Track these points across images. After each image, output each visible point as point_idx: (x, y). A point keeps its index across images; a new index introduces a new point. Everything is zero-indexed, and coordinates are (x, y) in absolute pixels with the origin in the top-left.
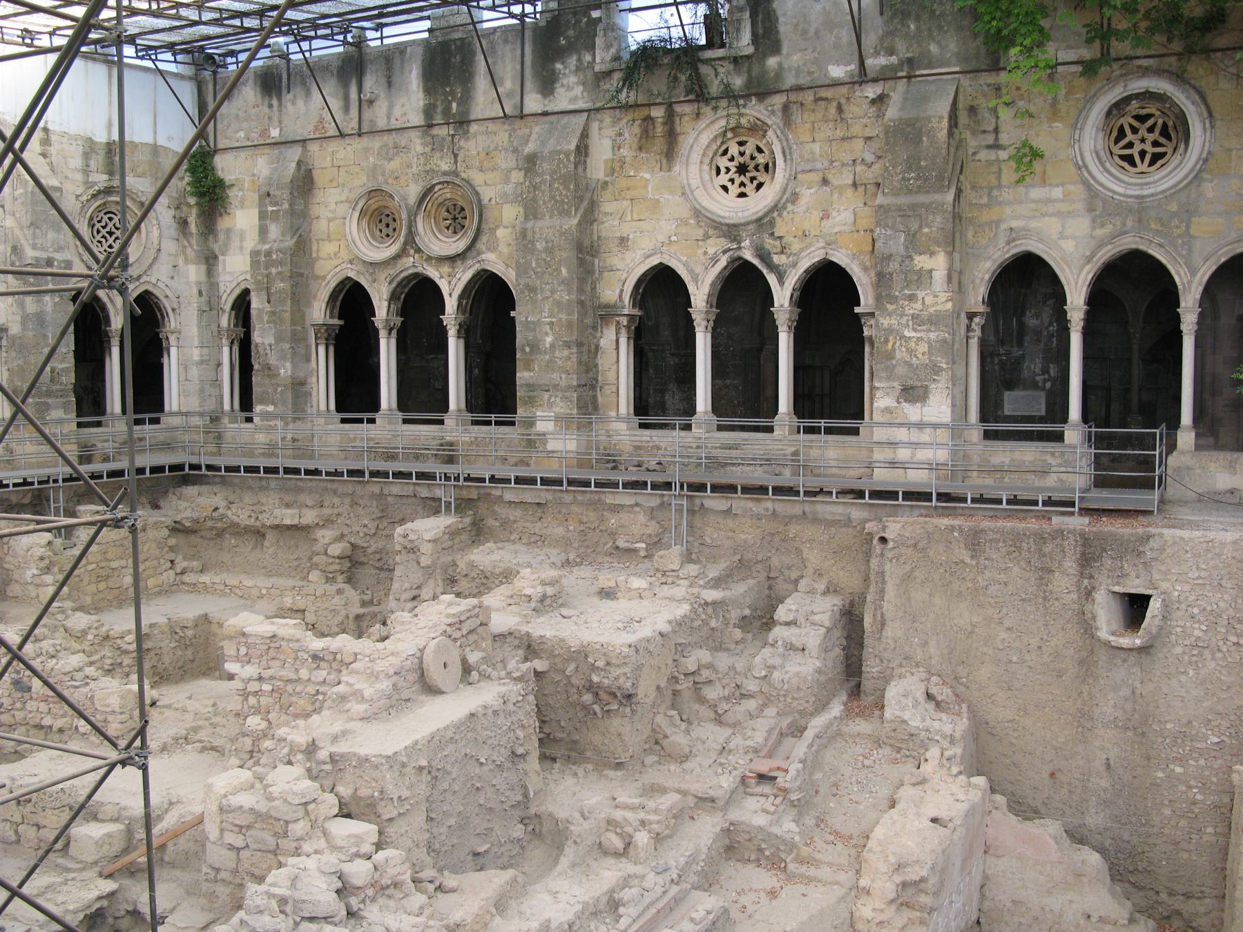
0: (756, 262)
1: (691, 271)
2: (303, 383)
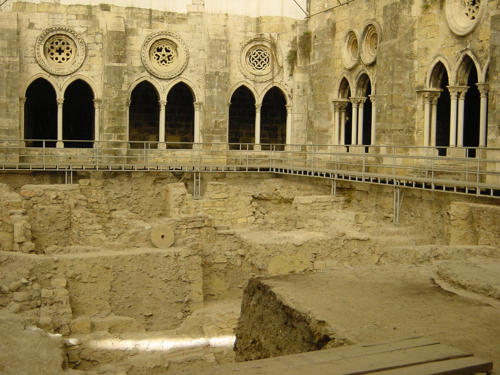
0: (472, 56)
1: (449, 64)
2: (325, 131)
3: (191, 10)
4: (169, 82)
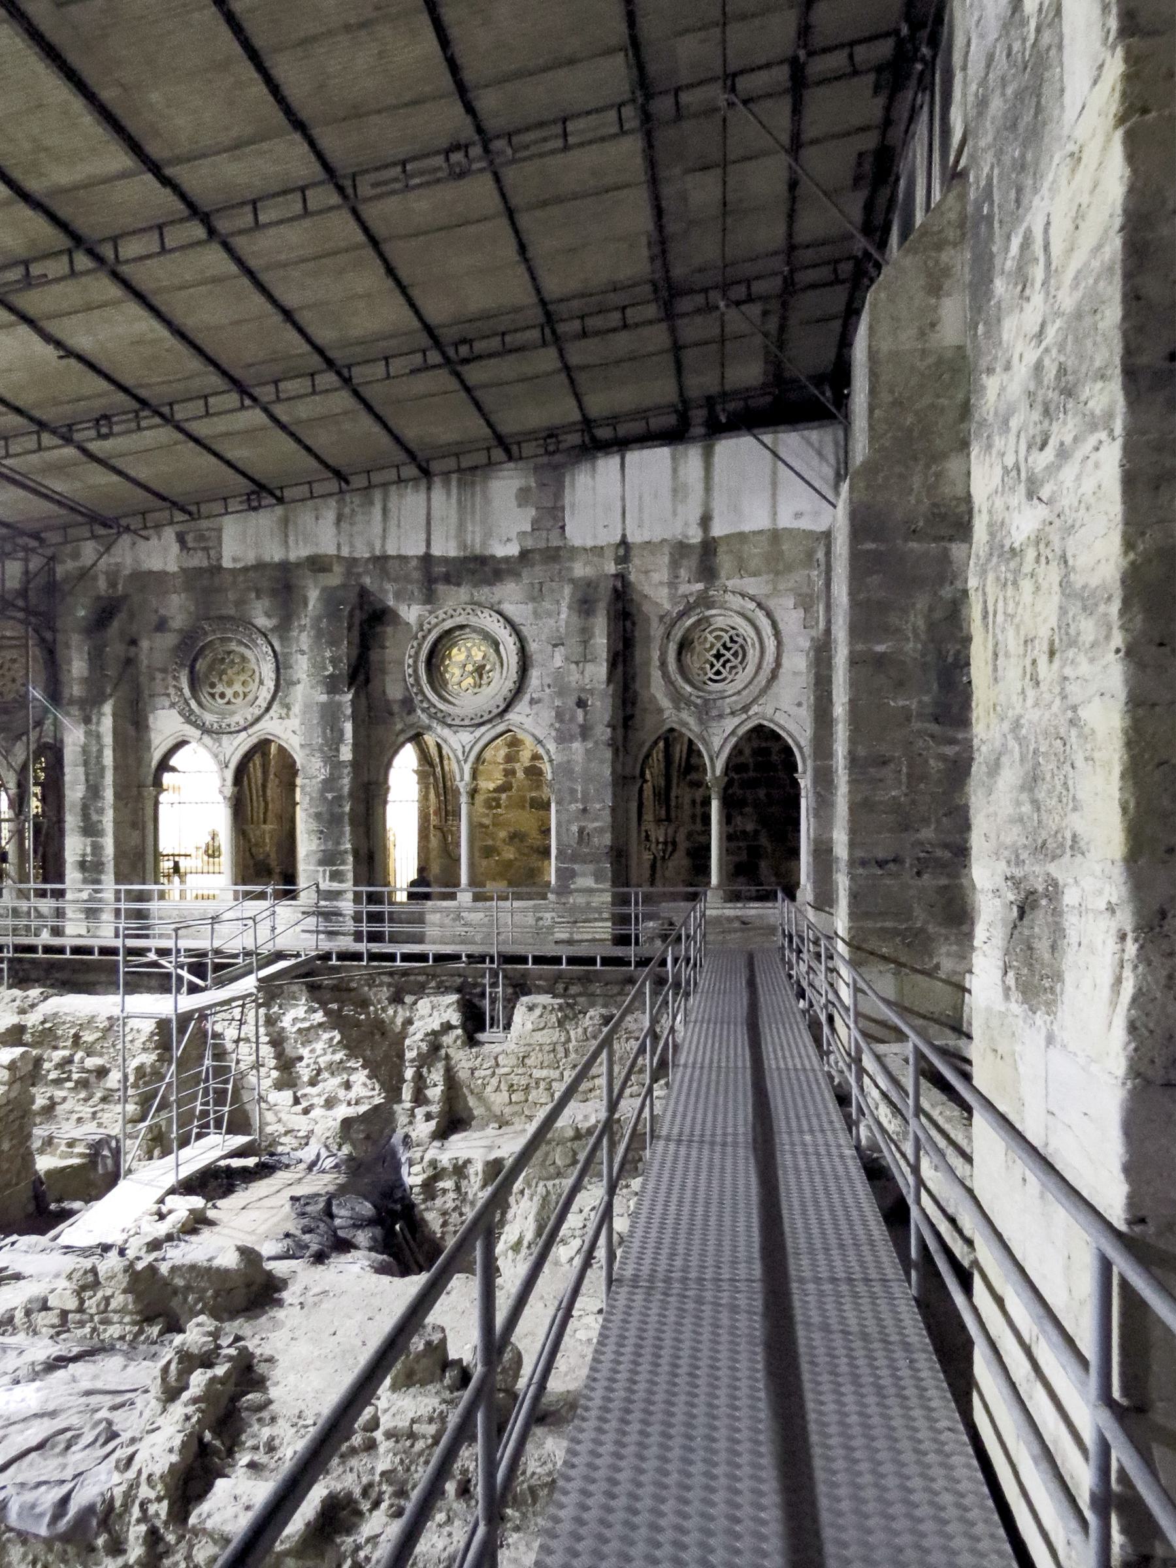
3: (529, 544)
4: (478, 732)
